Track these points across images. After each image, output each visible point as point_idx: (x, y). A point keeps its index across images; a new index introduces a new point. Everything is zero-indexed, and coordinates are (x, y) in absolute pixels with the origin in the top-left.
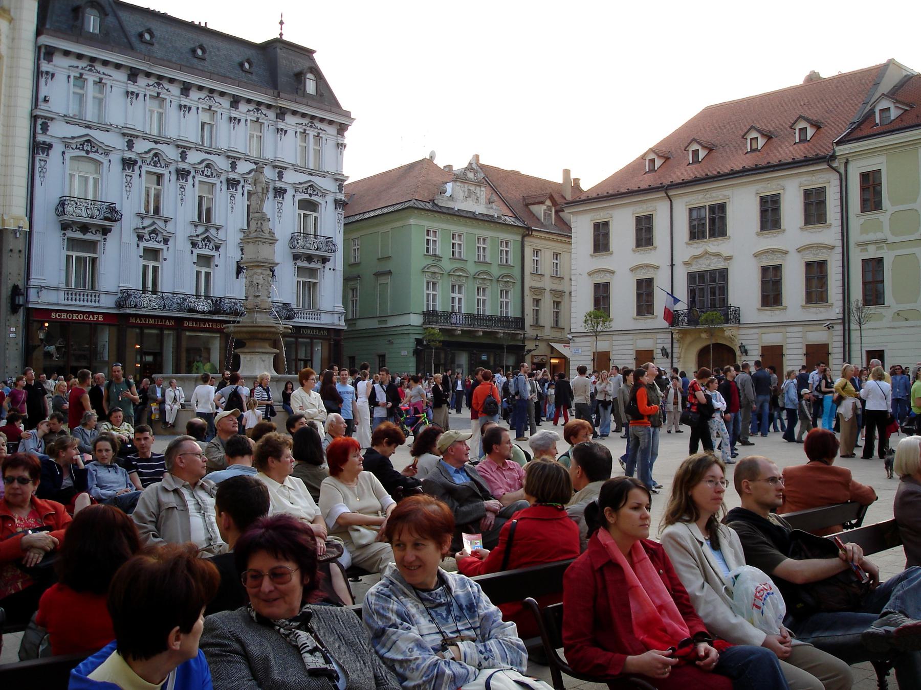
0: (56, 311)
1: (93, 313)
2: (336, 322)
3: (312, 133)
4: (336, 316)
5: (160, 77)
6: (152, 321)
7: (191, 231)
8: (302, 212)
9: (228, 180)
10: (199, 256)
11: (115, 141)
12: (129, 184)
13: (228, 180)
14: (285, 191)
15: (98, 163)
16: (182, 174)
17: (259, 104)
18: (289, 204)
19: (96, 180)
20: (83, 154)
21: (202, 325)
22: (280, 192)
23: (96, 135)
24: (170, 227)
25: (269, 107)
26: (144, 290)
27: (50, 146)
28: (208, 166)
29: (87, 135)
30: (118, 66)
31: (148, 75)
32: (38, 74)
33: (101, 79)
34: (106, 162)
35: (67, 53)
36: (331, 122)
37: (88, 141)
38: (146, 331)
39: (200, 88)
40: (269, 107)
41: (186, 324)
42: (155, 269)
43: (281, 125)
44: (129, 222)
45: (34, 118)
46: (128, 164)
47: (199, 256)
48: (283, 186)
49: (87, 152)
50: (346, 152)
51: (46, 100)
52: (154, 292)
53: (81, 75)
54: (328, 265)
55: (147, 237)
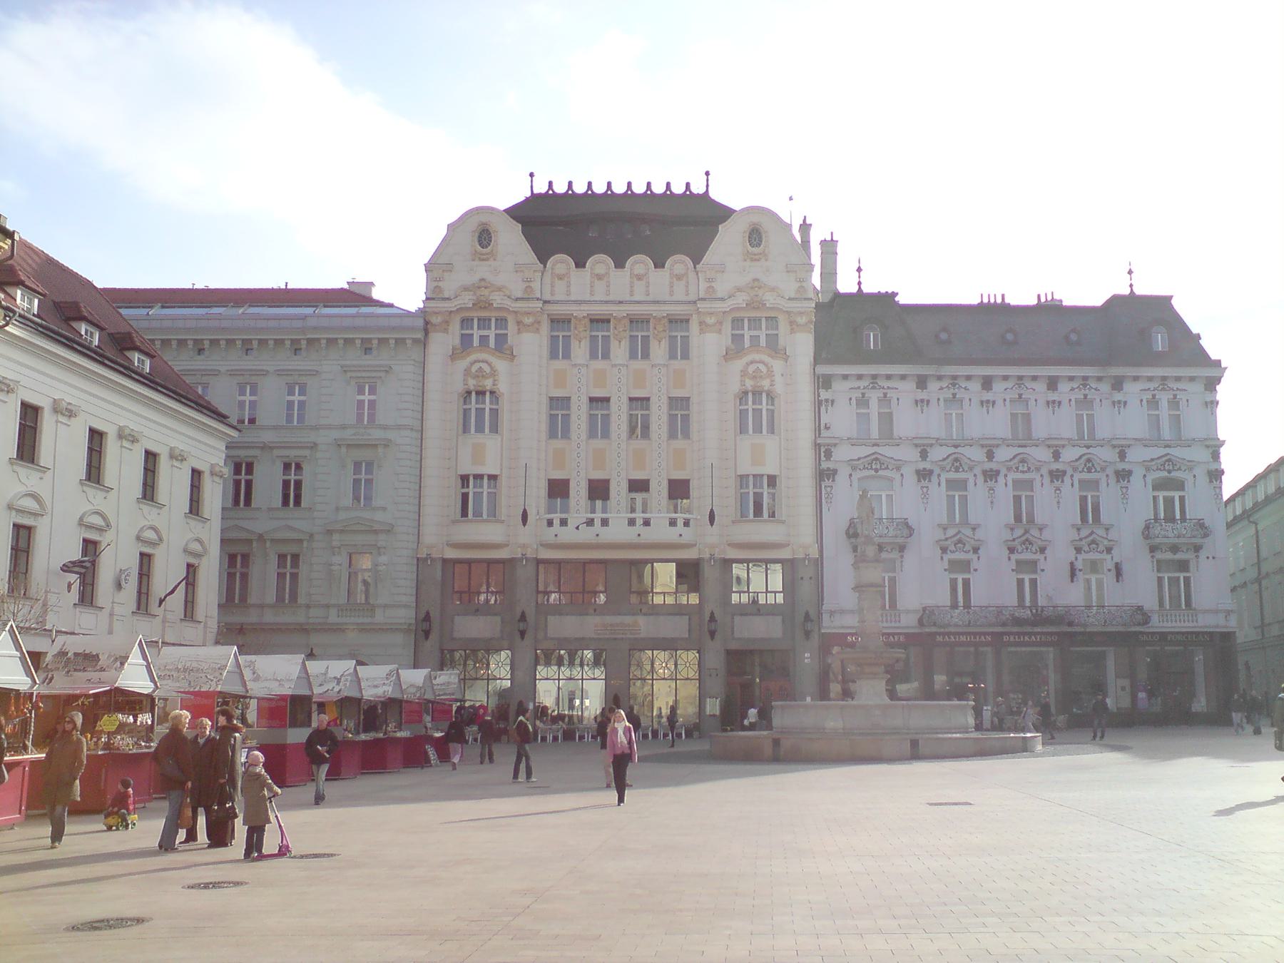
1: (893, 635)
2: (1222, 622)
3: (1164, 398)
4: (1222, 616)
5: (955, 378)
6: (963, 638)
7: (1007, 535)
8: (1161, 495)
9: (1051, 473)
10: (1018, 562)
11: (908, 454)
12: (925, 496)
13: (1051, 473)
14: (1130, 473)
15: (891, 480)
16: (991, 475)
17: (1085, 378)
18: (1140, 489)
19: (889, 497)
20: (873, 472)
22: (1124, 475)
23: (887, 451)
24: (980, 534)
25: (1099, 379)
26: (954, 606)
27: (835, 472)
28: (1023, 461)
30: (903, 377)
31: (940, 378)
32: (820, 403)
33: (885, 395)
34: (897, 476)
35: (845, 377)
36: (1192, 379)
37: (876, 459)
38: (957, 649)
39: (1006, 378)
40: (1099, 379)
41: (1006, 638)
42: (966, 583)
43: (1118, 396)
44: (927, 537)
45: (817, 446)
46: (924, 475)
47: (1018, 562)
48: (1127, 467)
49: (876, 471)
50: (1220, 411)
51: (827, 428)
52: (967, 605)
53: (863, 394)
54: (1203, 554)
55: (952, 548)
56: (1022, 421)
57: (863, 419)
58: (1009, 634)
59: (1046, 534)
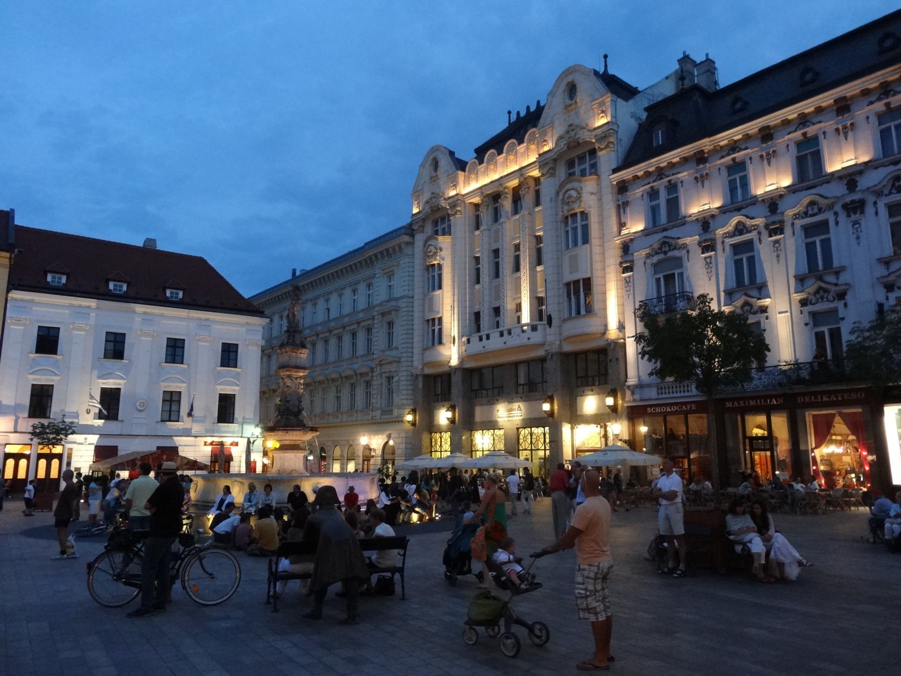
0: (651, 406)
1: (686, 403)
6: (752, 403)
9: (845, 207)
13: (845, 207)
15: (680, 259)
20: (662, 256)
21: (825, 399)
29: (665, 237)
41: (800, 400)
49: (665, 253)
56: (808, 162)
57: (654, 211)
58: (804, 394)
59: (844, 278)
